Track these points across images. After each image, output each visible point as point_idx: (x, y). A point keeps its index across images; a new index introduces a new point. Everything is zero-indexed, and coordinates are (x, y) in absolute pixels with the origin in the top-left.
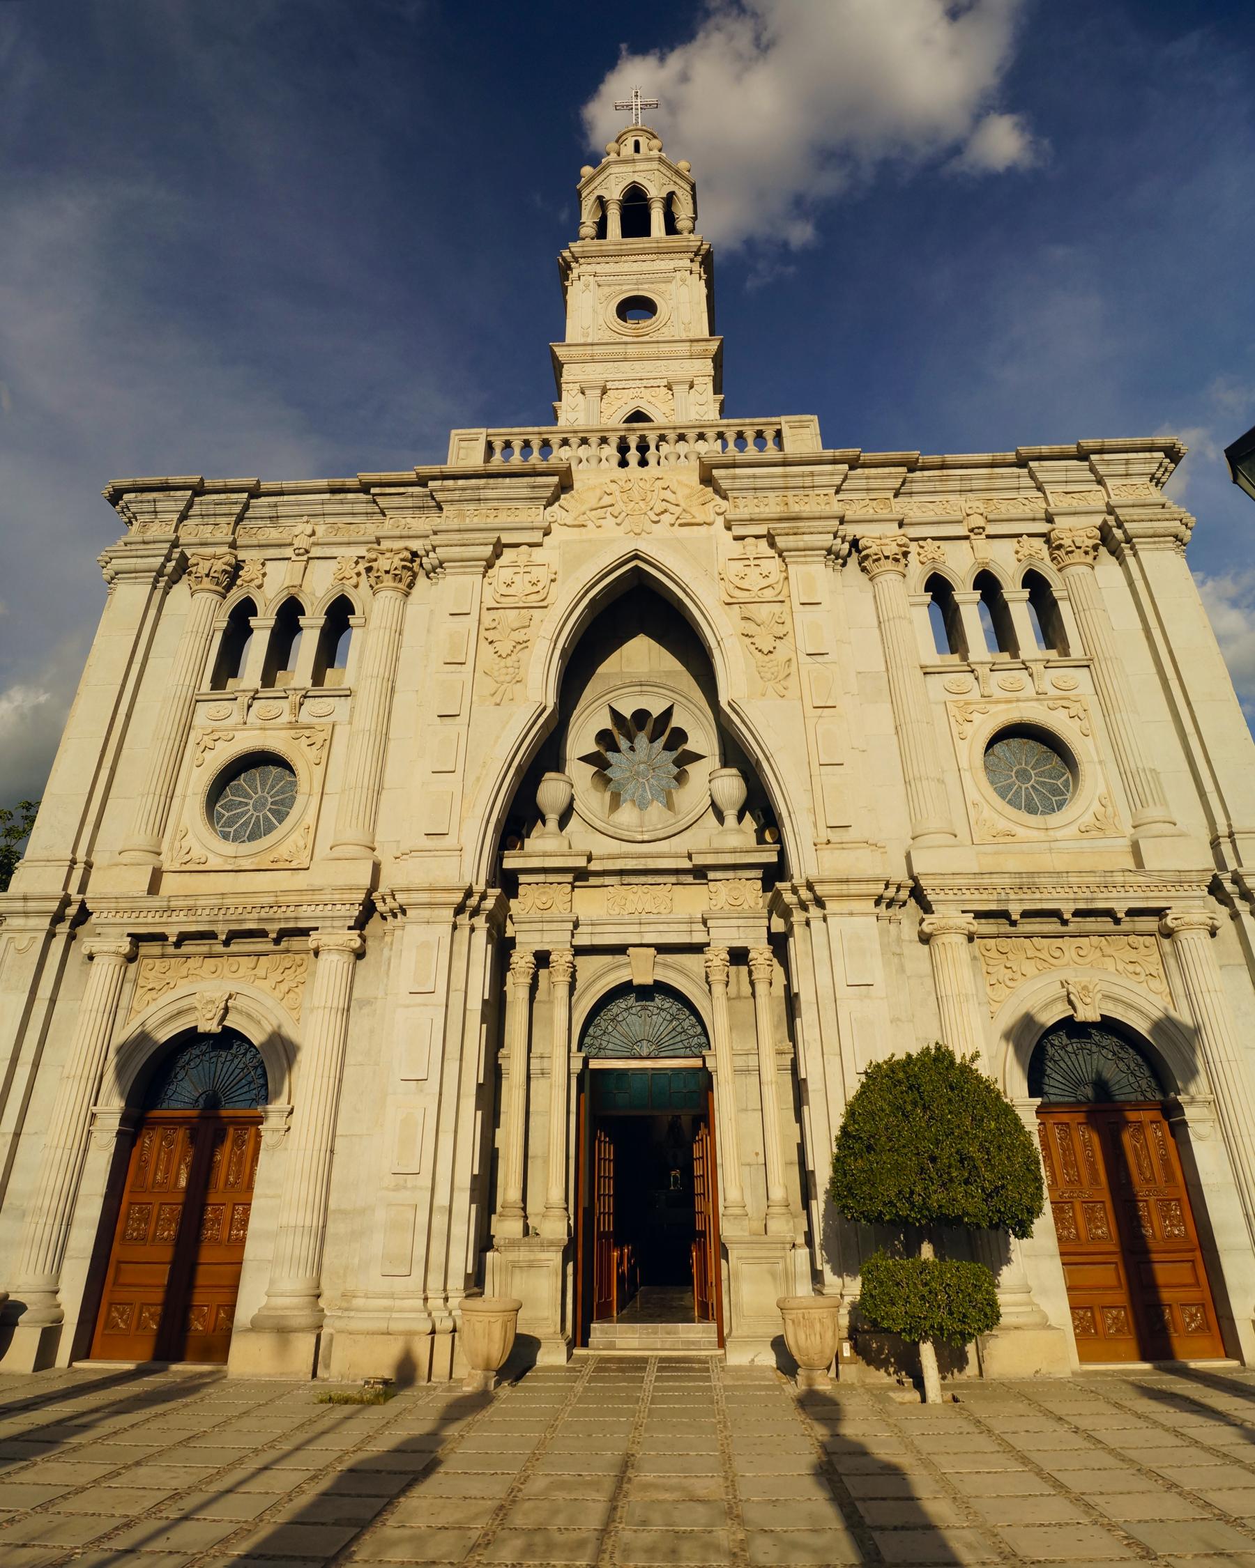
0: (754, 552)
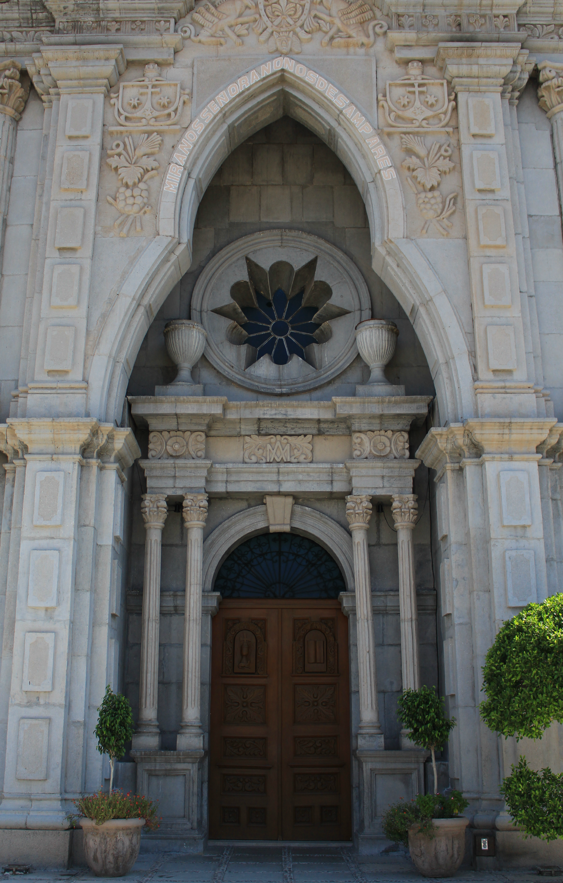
0: (419, 78)
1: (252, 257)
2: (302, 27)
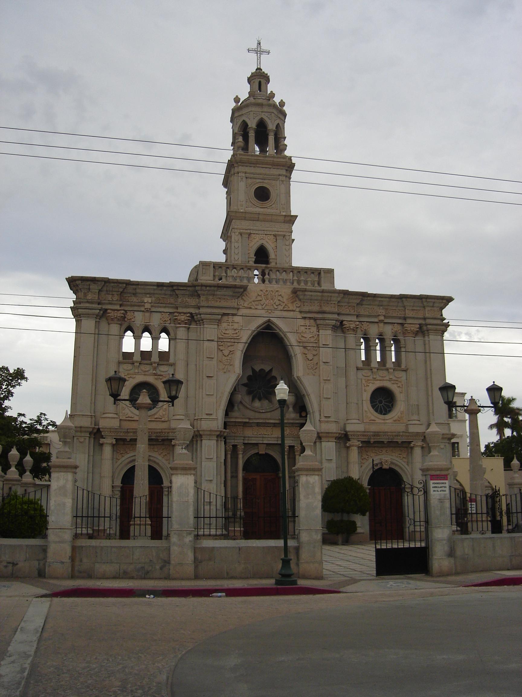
0: (309, 323)
1: (253, 367)
2: (275, 303)
